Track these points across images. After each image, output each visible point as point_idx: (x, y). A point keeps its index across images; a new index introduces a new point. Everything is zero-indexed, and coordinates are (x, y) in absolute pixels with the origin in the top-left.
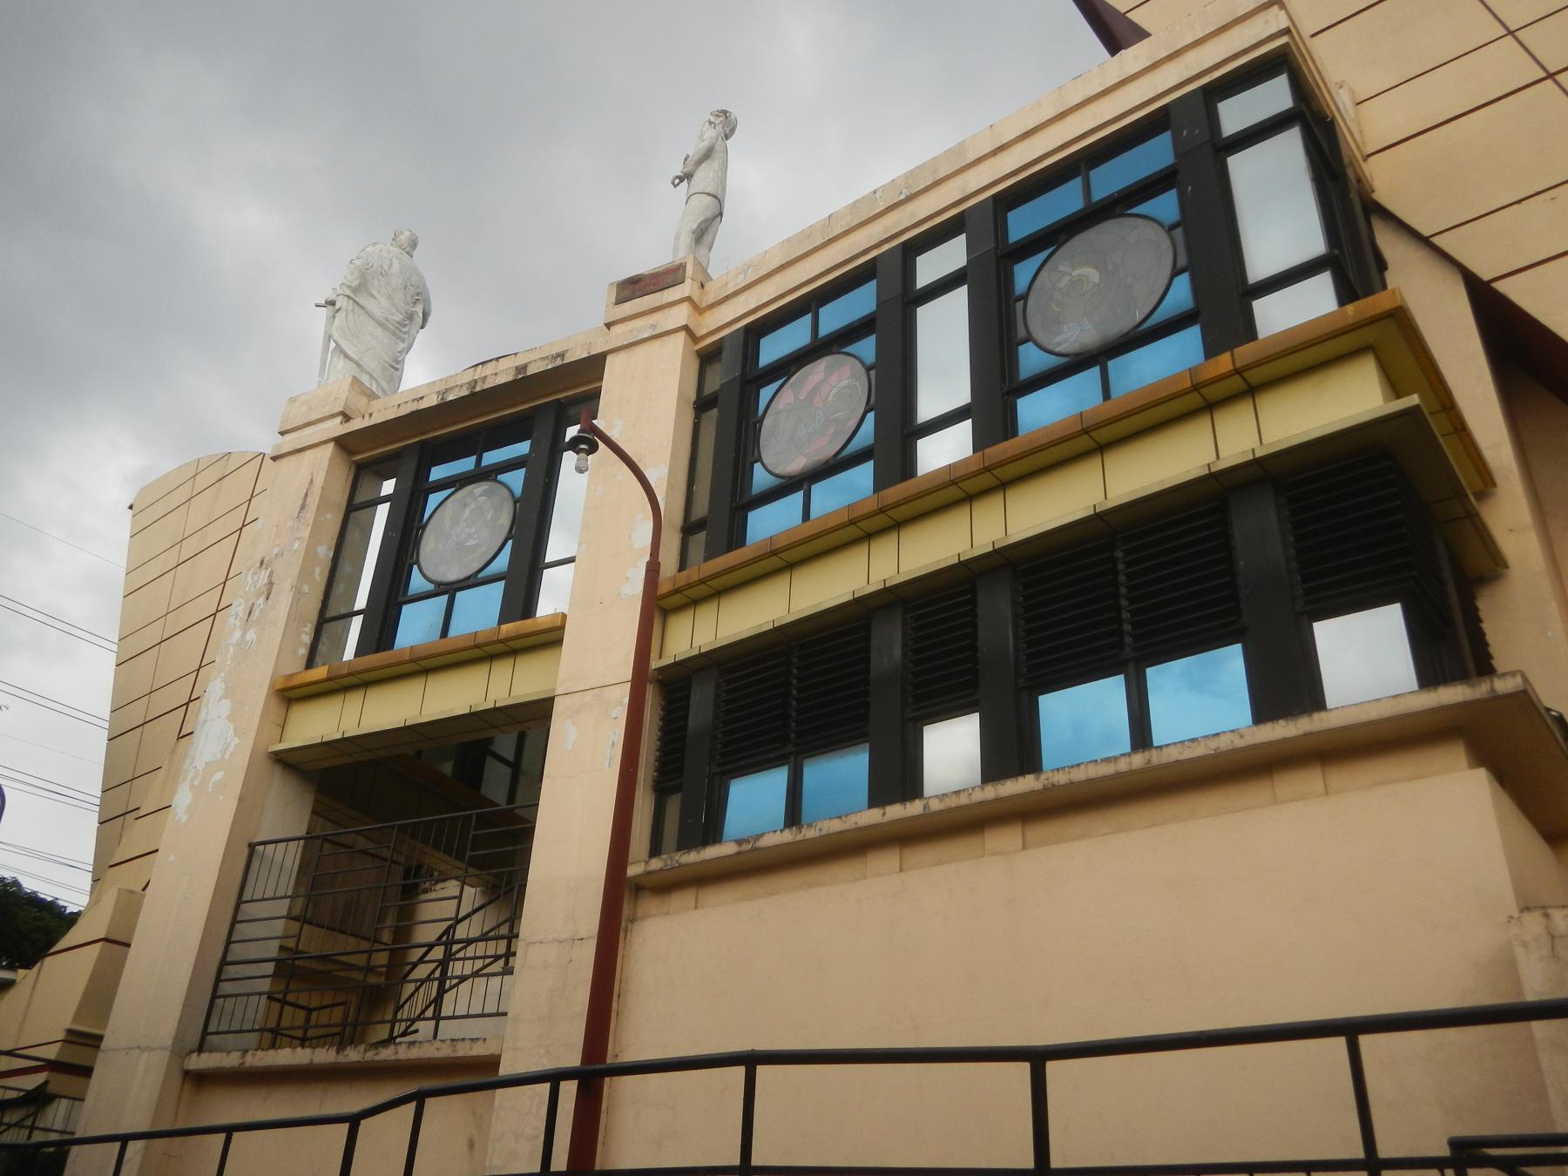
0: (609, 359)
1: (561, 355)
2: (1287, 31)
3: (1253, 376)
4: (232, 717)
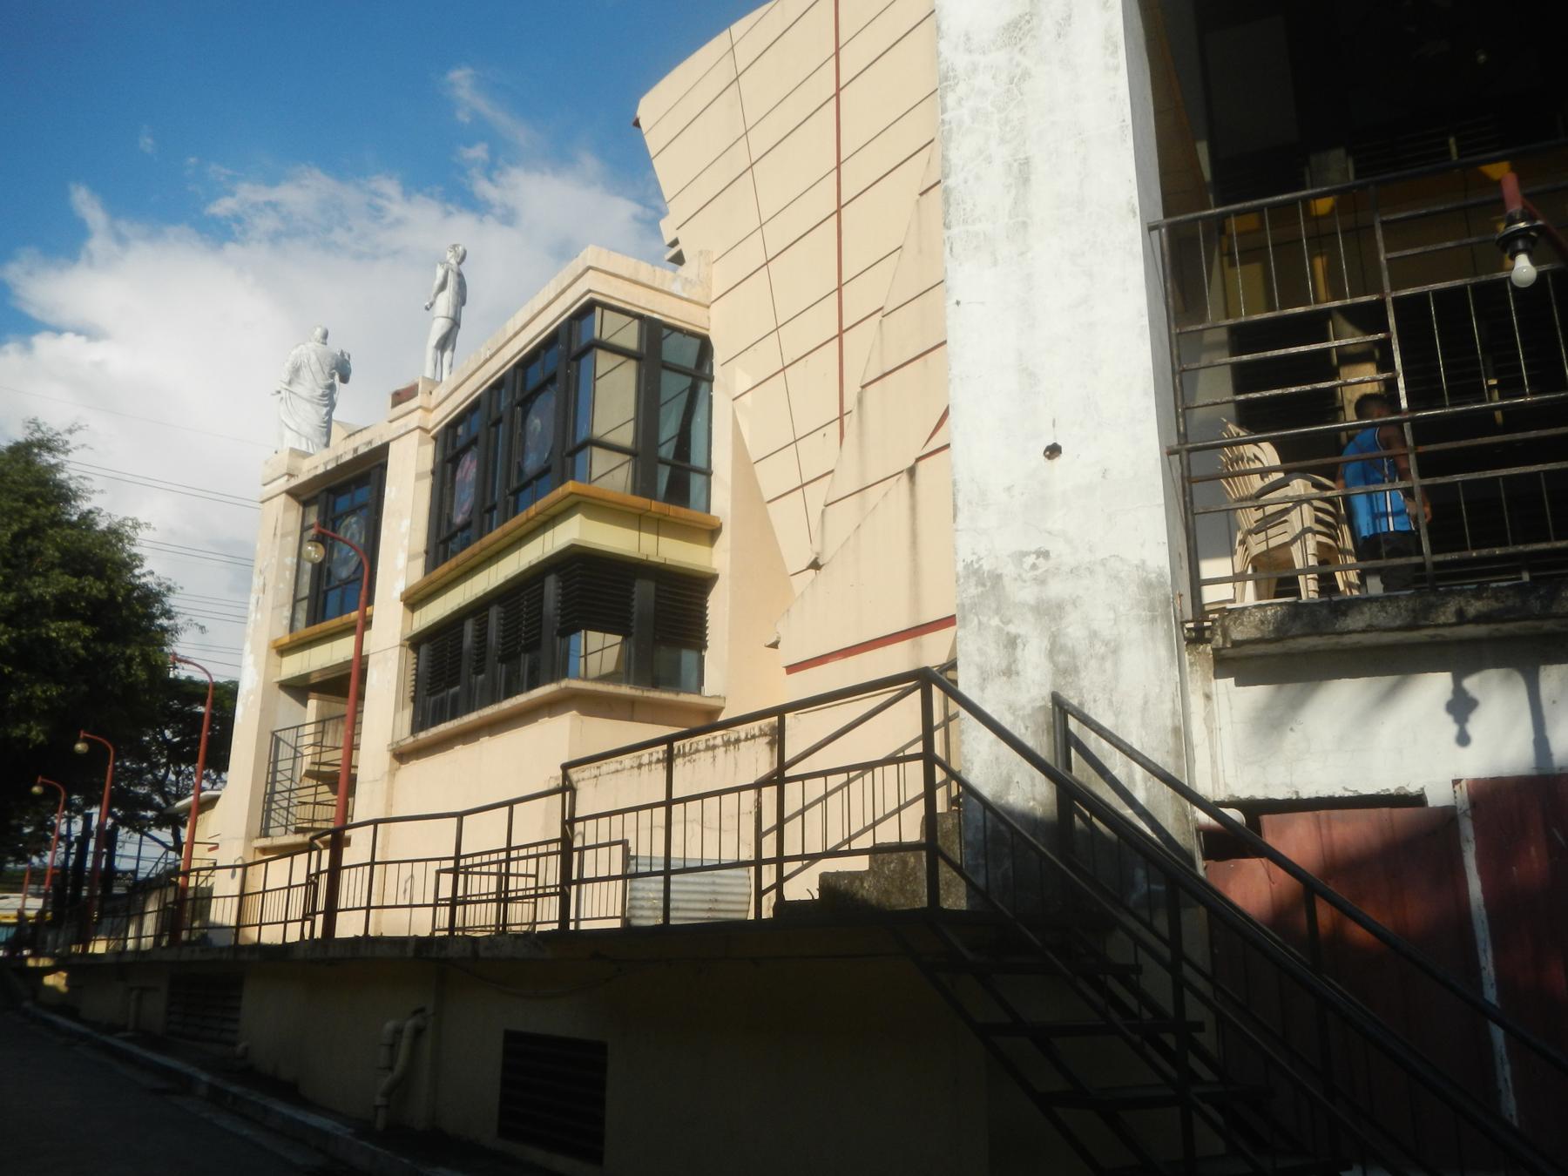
0: (392, 446)
2: (590, 291)
3: (553, 511)
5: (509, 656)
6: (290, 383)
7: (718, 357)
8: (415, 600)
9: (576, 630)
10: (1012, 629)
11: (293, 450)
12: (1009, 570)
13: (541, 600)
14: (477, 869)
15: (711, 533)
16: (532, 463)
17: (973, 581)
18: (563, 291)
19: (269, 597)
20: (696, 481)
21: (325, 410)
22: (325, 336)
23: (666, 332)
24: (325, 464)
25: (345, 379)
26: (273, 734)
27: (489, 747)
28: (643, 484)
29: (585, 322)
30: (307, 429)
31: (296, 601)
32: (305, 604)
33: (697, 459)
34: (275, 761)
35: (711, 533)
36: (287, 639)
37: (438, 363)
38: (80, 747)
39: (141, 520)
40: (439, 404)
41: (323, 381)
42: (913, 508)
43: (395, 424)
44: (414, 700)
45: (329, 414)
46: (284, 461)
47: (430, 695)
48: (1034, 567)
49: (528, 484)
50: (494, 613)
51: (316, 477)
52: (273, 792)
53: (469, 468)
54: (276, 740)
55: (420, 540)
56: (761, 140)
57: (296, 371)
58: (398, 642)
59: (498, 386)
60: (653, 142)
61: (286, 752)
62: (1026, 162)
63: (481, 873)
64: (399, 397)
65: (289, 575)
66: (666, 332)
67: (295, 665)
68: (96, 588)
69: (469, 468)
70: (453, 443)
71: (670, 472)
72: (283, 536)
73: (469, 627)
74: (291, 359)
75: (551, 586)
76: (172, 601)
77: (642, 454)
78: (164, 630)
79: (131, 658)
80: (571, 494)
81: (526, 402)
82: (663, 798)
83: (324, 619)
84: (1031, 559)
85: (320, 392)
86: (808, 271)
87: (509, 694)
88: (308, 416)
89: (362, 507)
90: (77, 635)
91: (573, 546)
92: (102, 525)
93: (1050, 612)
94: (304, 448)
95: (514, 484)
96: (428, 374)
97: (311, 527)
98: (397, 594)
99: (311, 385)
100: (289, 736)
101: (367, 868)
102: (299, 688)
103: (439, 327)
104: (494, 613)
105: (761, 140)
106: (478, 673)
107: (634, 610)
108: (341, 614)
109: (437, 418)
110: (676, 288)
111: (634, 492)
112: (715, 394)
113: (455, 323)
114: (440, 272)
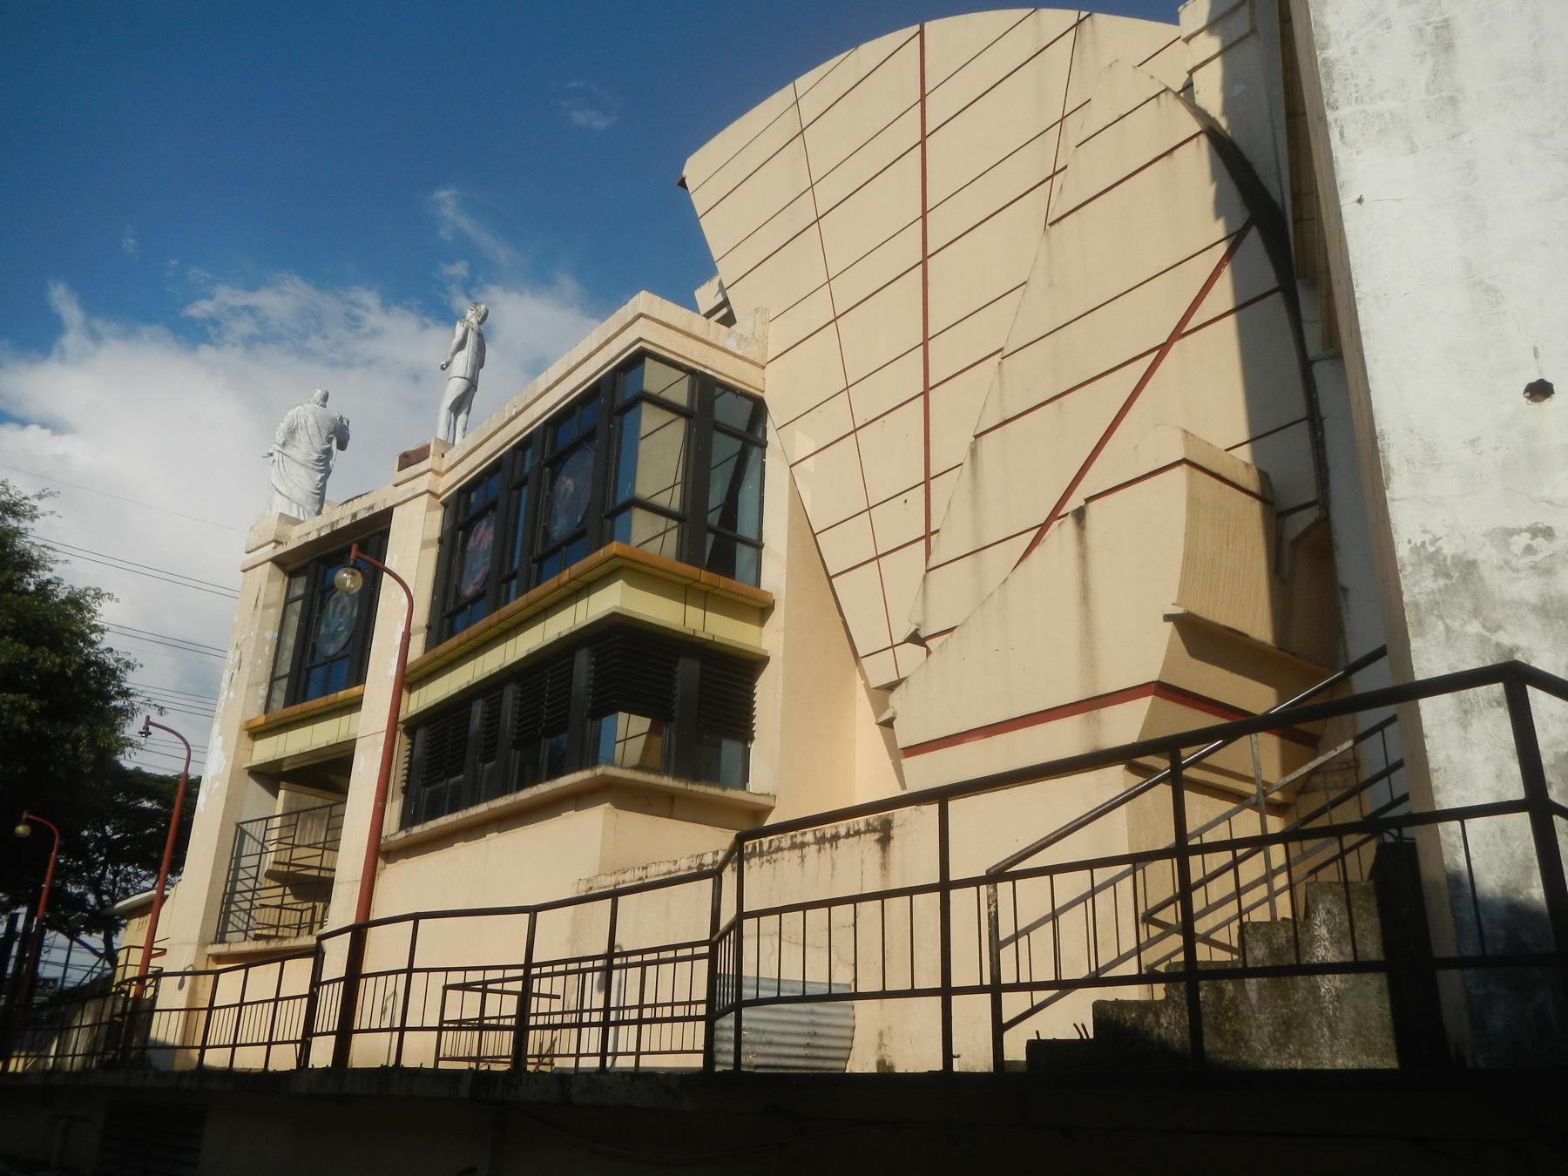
1: (372, 507)
2: (640, 339)
3: (587, 578)
4: (224, 748)
5: (527, 740)
6: (284, 445)
7: (774, 419)
8: (409, 679)
9: (612, 710)
11: (282, 515)
12: (1487, 555)
13: (571, 677)
14: (498, 986)
15: (761, 610)
16: (560, 527)
17: (1428, 570)
18: (608, 342)
19: (245, 675)
20: (744, 554)
21: (319, 476)
22: (325, 398)
23: (718, 391)
24: (319, 530)
25: (342, 446)
26: (238, 825)
27: (496, 844)
28: (689, 551)
29: (633, 374)
30: (299, 495)
31: (274, 680)
32: (284, 683)
33: (745, 528)
34: (237, 856)
35: (761, 610)
36: (262, 720)
37: (452, 426)
38: (21, 829)
39: (104, 591)
40: (453, 467)
41: (319, 445)
42: (1083, 557)
43: (400, 488)
45: (324, 480)
46: (271, 527)
47: (426, 785)
48: (1529, 550)
49: (557, 549)
50: (510, 694)
51: (307, 544)
52: (234, 892)
53: (484, 536)
54: (241, 834)
56: (827, 194)
57: (292, 432)
59: (523, 446)
60: (700, 202)
61: (250, 846)
62: (1446, 24)
63: (502, 992)
64: (407, 460)
65: (268, 651)
66: (718, 391)
67: (269, 750)
68: (49, 660)
69: (484, 536)
70: (465, 510)
71: (717, 542)
72: (265, 607)
73: (478, 708)
74: (287, 419)
75: (583, 660)
76: (131, 680)
77: (689, 519)
78: (120, 711)
79: (78, 739)
80: (616, 556)
81: (556, 463)
82: (936, 879)
83: (304, 699)
84: (1525, 539)
85: (316, 456)
86: (889, 325)
87: (521, 786)
88: (302, 481)
90: (23, 709)
91: (614, 615)
92: (62, 595)
94: (294, 514)
95: (539, 550)
96: (441, 435)
97: (296, 599)
99: (307, 447)
100: (256, 830)
101: (403, 977)
102: (269, 776)
103: (455, 388)
104: (510, 694)
105: (827, 194)
106: (486, 760)
107: (677, 691)
108: (325, 693)
110: (731, 344)
111: (680, 557)
112: (767, 460)
113: (472, 385)
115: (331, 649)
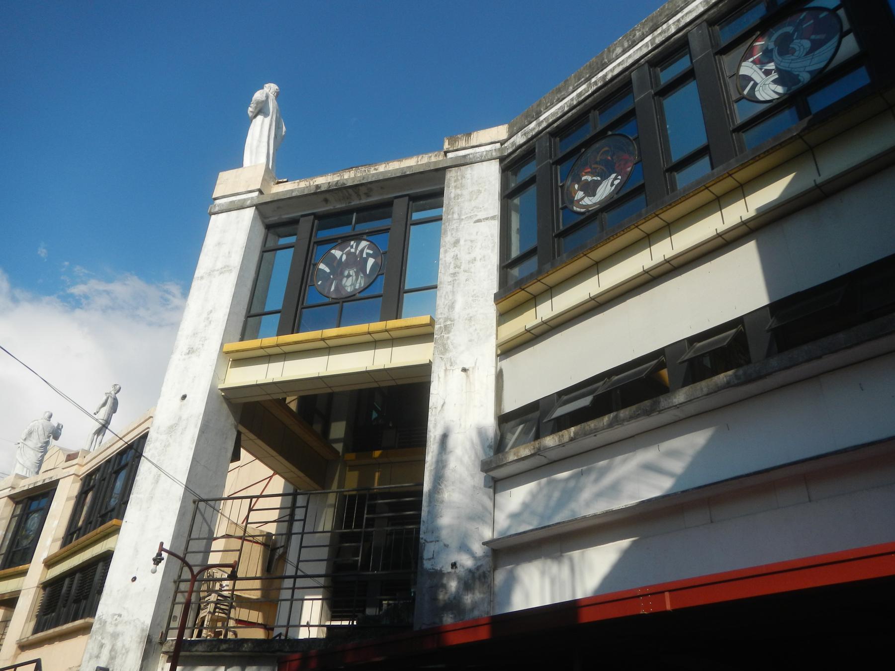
5: (77, 601)
6: (25, 440)
8: (50, 563)
10: (103, 641)
11: (17, 475)
12: (109, 620)
22: (50, 416)
25: (56, 438)
30: (28, 464)
41: (43, 439)
44: (37, 616)
45: (43, 457)
46: (9, 480)
55: (61, 532)
57: (30, 434)
58: (36, 585)
59: (109, 461)
73: (67, 581)
74: (29, 428)
81: (117, 473)
85: (40, 445)
88: (31, 456)
89: (41, 509)
93: (115, 636)
94: (24, 474)
95: (103, 512)
96: (87, 448)
98: (42, 560)
99: (36, 441)
106: (64, 607)
109: (84, 470)
114: (105, 398)
115: (25, 543)
